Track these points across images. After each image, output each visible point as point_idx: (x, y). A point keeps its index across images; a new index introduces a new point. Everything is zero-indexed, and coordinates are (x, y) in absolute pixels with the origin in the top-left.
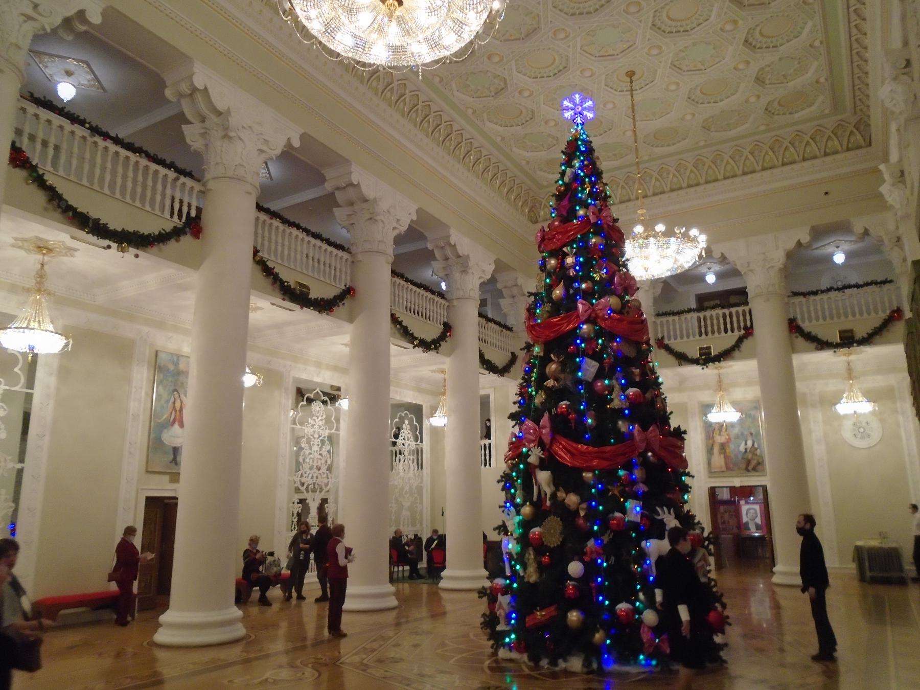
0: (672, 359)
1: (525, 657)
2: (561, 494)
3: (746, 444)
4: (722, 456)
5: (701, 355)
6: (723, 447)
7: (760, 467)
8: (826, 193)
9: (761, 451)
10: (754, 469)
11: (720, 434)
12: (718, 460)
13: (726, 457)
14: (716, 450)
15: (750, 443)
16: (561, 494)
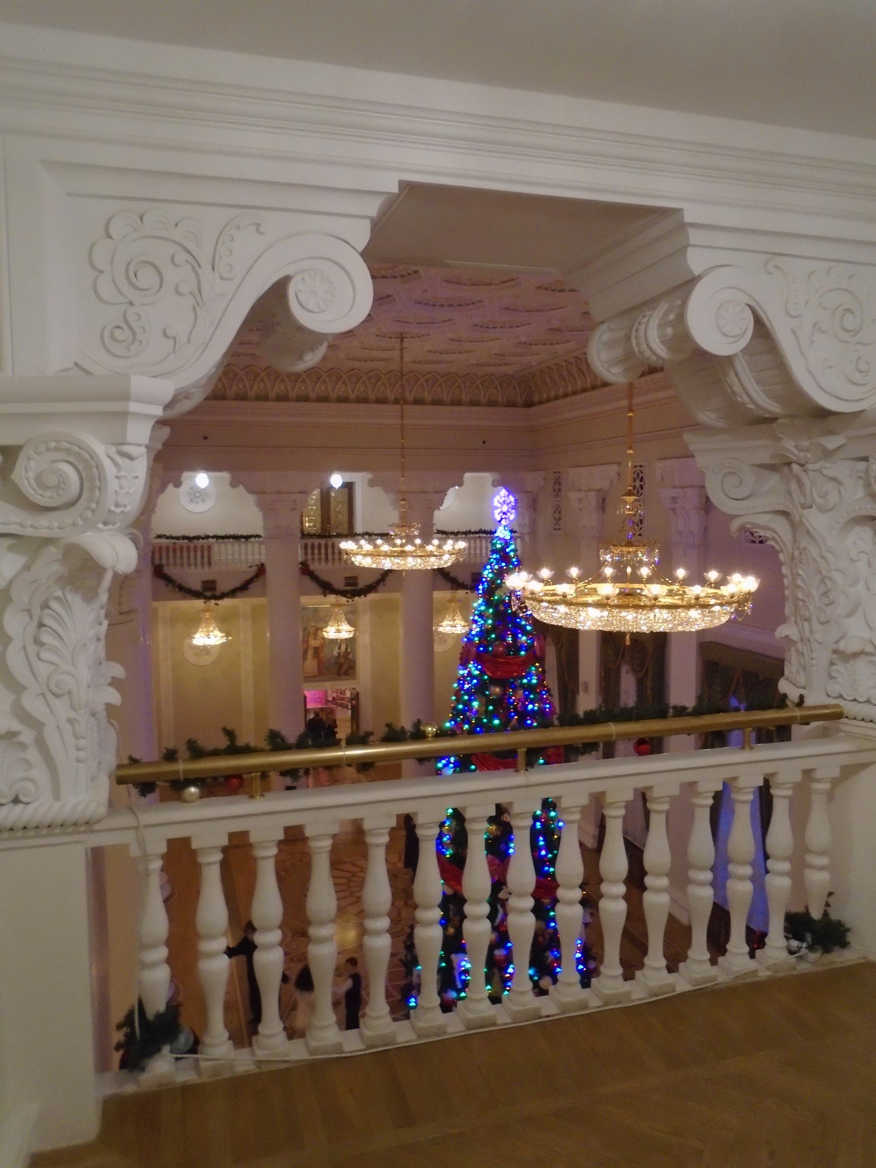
0: (313, 585)
3: (340, 649)
4: (316, 661)
5: (347, 585)
6: (317, 651)
8: (484, 442)
9: (354, 656)
10: (346, 673)
11: (315, 638)
12: (311, 664)
13: (320, 664)
15: (343, 647)
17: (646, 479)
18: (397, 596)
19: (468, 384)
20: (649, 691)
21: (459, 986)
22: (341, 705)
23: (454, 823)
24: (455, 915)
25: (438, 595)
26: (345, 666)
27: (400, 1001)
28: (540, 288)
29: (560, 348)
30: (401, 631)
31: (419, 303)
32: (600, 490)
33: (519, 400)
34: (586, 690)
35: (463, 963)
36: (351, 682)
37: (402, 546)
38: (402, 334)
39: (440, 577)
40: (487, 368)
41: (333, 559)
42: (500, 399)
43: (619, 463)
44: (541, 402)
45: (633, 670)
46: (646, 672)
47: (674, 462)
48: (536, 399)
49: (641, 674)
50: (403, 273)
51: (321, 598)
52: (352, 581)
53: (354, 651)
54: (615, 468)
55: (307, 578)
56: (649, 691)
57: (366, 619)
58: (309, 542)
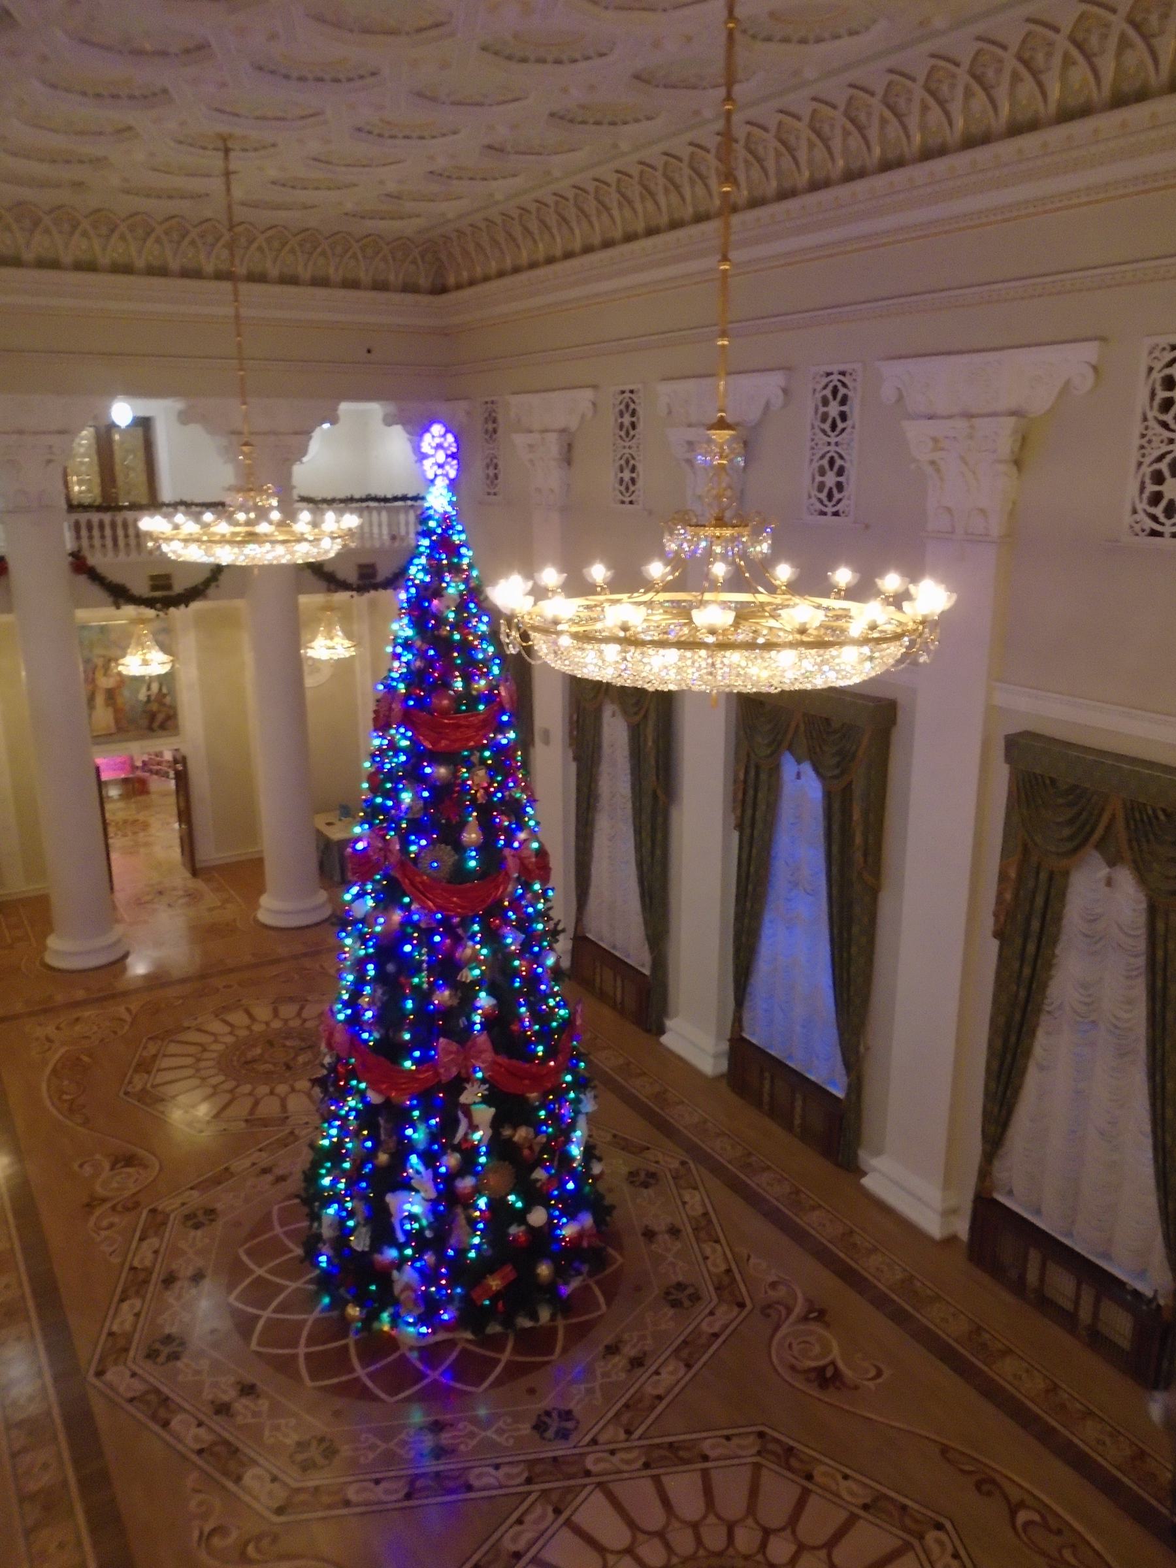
1: (469, 1336)
2: (507, 1132)
3: (149, 689)
4: (110, 710)
5: (154, 588)
6: (111, 695)
7: (169, 723)
8: (369, 351)
9: (174, 699)
10: (163, 727)
12: (103, 716)
13: (117, 711)
14: (100, 700)
15: (155, 687)
16: (507, 1132)
17: (640, 412)
18: (239, 603)
20: (650, 744)
21: (401, 1238)
22: (157, 773)
23: (379, 992)
24: (390, 1137)
25: (303, 599)
26: (160, 717)
27: (302, 1261)
28: (484, 49)
29: (500, 188)
30: (248, 657)
31: (260, 68)
32: (563, 431)
33: (424, 282)
34: (547, 742)
35: (407, 1207)
36: (172, 740)
37: (248, 523)
38: (224, 139)
39: (308, 573)
41: (127, 545)
42: (392, 278)
43: (595, 387)
44: (459, 287)
45: (625, 713)
46: (645, 716)
47: (690, 385)
49: (637, 718)
51: (111, 611)
52: (161, 581)
53: (172, 691)
54: (588, 394)
55: (82, 579)
56: (650, 744)
57: (188, 641)
58: (83, 517)
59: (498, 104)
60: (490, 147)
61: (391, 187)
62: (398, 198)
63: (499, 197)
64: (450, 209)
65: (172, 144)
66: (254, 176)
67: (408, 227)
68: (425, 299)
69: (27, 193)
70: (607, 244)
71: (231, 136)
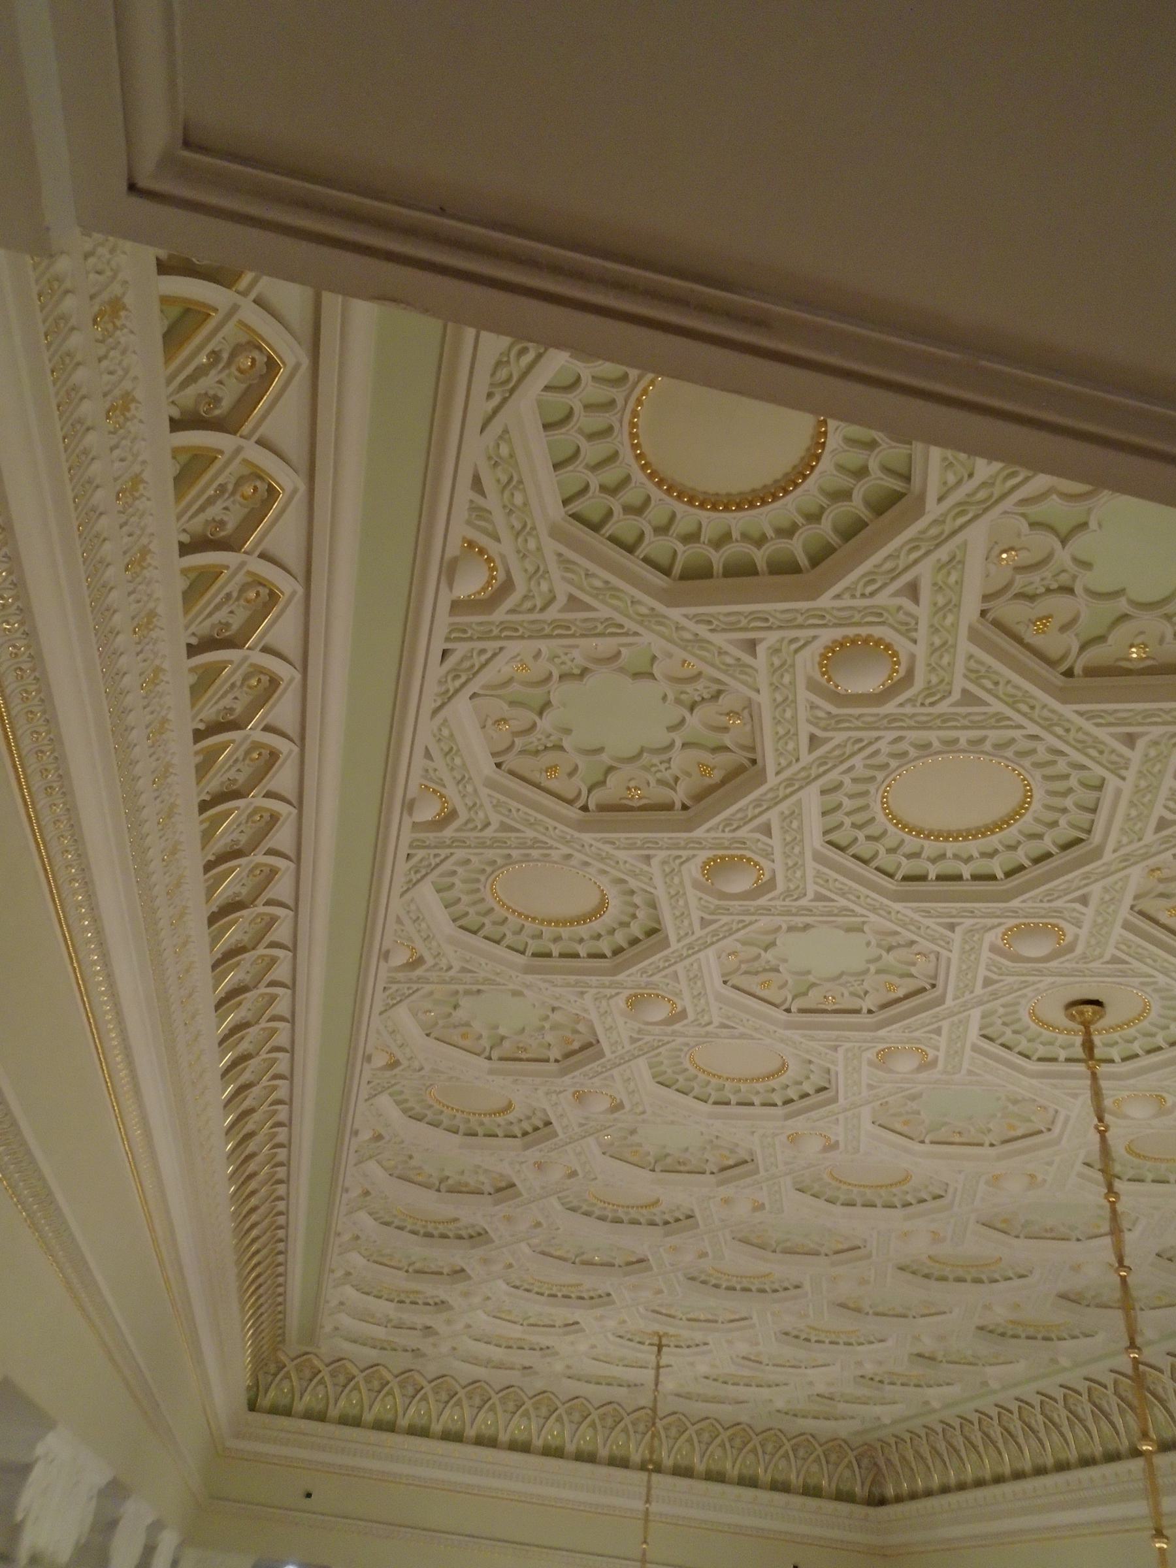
19: (770, 1448)
28: (902, 1269)
29: (935, 1396)
31: (693, 1279)
40: (801, 1422)
44: (899, 1499)
48: (890, 1491)
50: (667, 1217)
59: (922, 1316)
60: (920, 1355)
61: (821, 1388)
62: (831, 1399)
63: (936, 1404)
64: (886, 1413)
65: (611, 1338)
66: (685, 1371)
67: (844, 1429)
68: (860, 1510)
69: (480, 1372)
70: (1062, 1467)
71: (666, 1334)
